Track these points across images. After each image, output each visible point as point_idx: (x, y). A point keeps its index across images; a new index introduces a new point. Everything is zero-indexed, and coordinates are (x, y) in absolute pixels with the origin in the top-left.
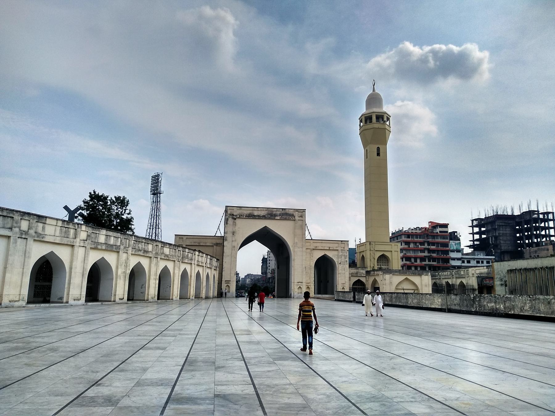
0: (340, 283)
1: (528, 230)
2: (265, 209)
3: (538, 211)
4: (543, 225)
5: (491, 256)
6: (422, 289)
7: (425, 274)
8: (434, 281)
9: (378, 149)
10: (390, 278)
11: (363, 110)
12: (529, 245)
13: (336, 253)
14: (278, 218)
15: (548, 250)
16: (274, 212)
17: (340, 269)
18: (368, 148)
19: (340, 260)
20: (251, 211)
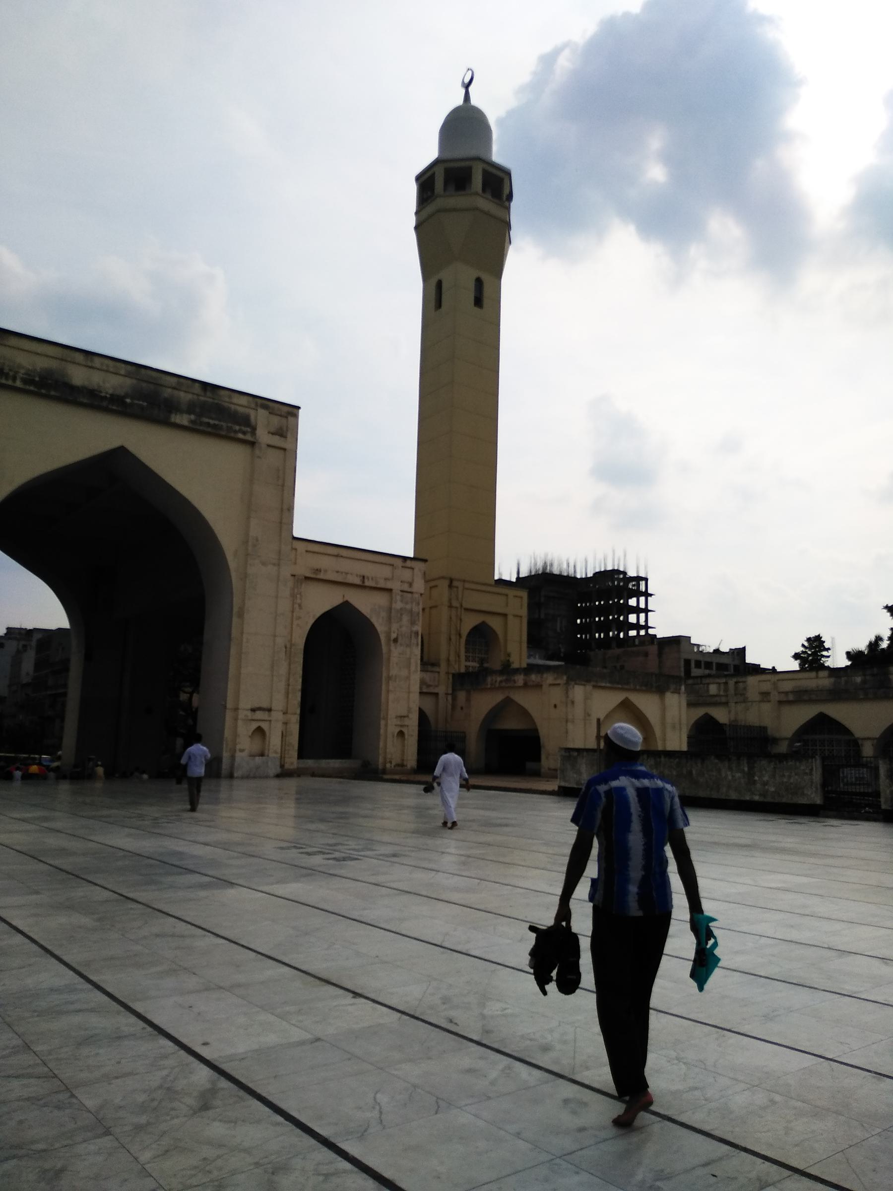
0: (392, 714)
1: (601, 611)
2: (123, 369)
3: (624, 573)
4: (632, 602)
5: (558, 660)
6: (664, 740)
7: (672, 687)
8: (700, 712)
9: (479, 282)
10: (586, 698)
11: (428, 151)
12: (606, 643)
13: (381, 599)
14: (183, 419)
15: (646, 655)
16: (167, 393)
17: (394, 659)
18: (445, 275)
19: (395, 627)
20: (53, 364)
